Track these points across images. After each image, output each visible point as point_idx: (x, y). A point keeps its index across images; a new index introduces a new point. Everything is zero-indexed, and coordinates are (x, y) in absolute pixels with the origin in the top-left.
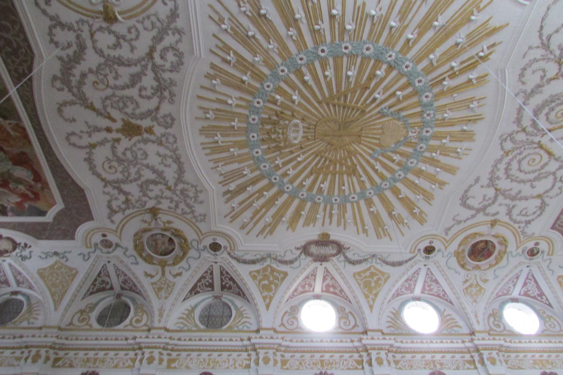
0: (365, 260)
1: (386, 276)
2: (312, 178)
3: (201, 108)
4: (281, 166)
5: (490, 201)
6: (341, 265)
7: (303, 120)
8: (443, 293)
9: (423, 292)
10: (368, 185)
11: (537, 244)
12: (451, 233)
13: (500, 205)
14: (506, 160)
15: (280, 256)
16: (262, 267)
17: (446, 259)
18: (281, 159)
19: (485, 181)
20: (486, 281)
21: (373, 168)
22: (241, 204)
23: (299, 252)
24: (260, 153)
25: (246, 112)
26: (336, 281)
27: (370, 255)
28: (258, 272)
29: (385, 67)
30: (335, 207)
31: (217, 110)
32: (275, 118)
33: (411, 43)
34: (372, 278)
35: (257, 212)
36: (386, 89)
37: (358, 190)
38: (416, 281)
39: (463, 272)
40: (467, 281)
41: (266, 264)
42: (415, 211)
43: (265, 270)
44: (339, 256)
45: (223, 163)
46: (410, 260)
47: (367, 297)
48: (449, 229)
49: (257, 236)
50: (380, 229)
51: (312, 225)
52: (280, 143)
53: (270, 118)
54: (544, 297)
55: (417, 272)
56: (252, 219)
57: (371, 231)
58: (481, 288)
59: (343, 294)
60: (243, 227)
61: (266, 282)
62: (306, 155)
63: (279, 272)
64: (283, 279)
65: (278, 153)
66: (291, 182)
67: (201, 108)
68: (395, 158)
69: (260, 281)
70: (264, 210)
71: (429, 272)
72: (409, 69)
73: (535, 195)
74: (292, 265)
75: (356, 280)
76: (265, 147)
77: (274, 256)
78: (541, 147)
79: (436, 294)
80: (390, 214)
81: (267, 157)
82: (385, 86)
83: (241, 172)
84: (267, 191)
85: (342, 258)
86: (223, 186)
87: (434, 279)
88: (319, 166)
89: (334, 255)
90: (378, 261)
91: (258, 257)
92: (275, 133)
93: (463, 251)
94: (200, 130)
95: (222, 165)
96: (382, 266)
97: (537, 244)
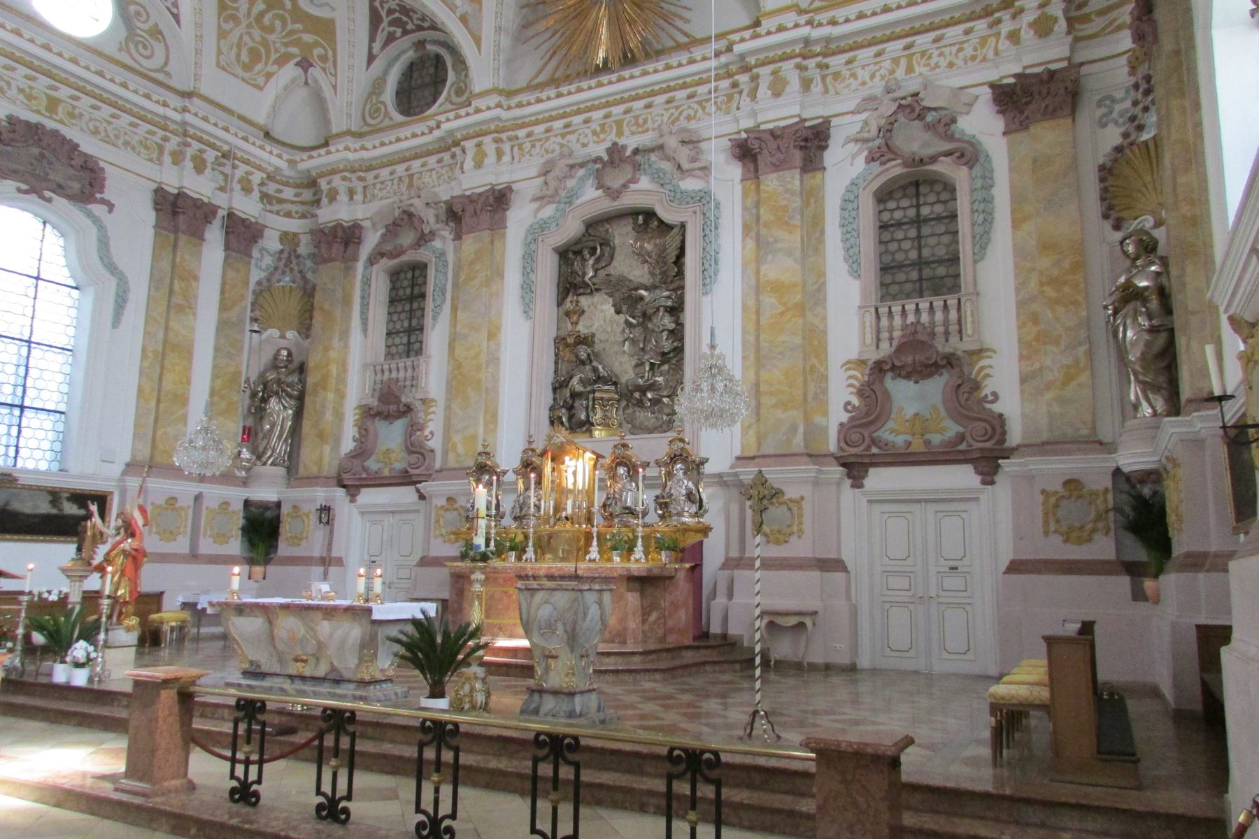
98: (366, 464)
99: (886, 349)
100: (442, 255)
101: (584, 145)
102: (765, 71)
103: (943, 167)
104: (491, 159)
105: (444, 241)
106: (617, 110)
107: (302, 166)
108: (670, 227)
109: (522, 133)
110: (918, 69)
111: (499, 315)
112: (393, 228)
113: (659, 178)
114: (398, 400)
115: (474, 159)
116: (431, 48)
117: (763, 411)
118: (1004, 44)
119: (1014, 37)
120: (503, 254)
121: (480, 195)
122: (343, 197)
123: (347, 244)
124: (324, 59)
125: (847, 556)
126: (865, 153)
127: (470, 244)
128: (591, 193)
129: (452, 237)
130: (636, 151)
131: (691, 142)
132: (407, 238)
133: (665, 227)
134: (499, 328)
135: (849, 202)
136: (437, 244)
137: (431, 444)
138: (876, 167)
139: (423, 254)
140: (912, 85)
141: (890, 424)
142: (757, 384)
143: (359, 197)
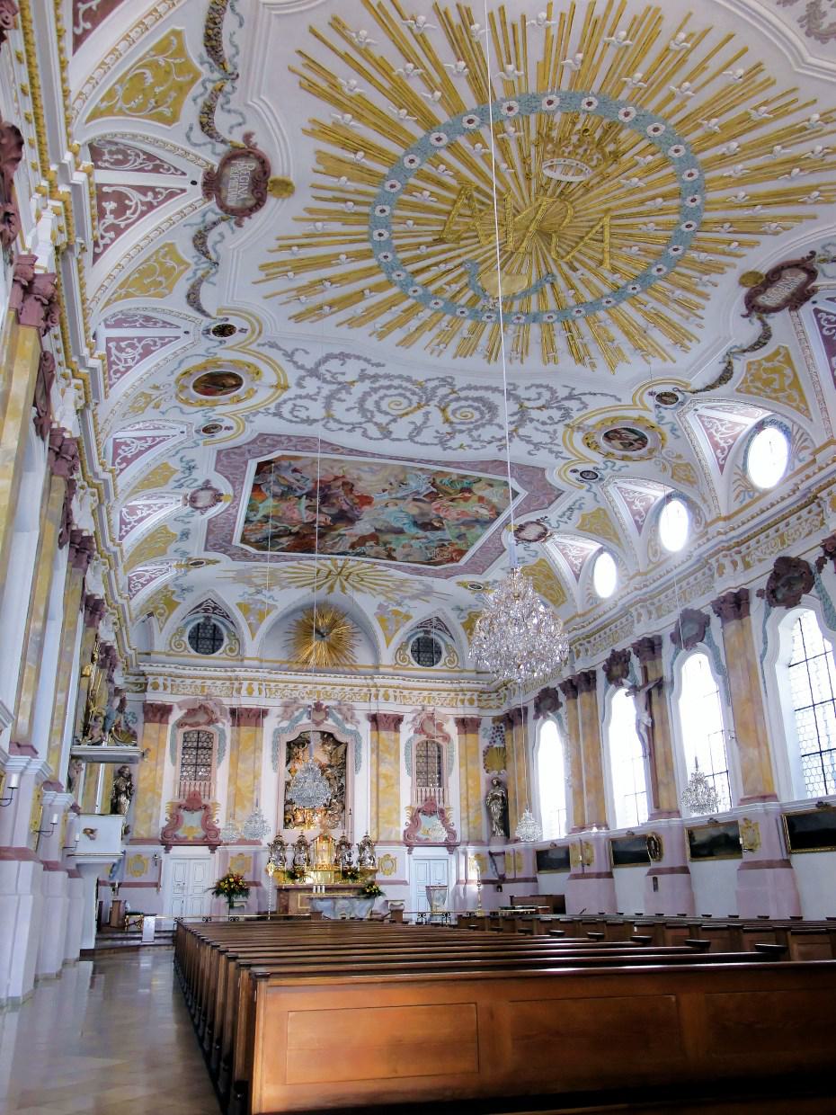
0: (206, 254)
1: (167, 291)
2: (453, 182)
3: (706, 32)
4: (499, 136)
5: (329, 379)
6: (196, 218)
7: (587, 188)
8: (123, 370)
9: (109, 340)
10: (401, 256)
11: (228, 428)
12: (266, 351)
13: (319, 388)
14: (405, 384)
15: (228, 102)
16: (196, 62)
17: (203, 353)
18: (518, 139)
19: (371, 371)
20: (156, 407)
21: (445, 261)
22: (422, 40)
23: (241, 143)
24: (545, 107)
25: (650, 107)
26: (143, 214)
27: (218, 258)
28: (181, 51)
29: (622, 283)
30: (366, 209)
31: (682, 61)
32: (610, 148)
33: (642, 307)
34: (160, 275)
35: (384, 69)
36: (586, 283)
37: (396, 242)
38: (143, 326)
39: (174, 378)
40: (156, 388)
41: (204, 71)
42: (326, 309)
43: (186, 68)
44: (218, 210)
45: (554, 32)
46: (203, 312)
47: (121, 286)
48: (273, 345)
49: (300, 52)
50: (289, 268)
51: (321, 168)
52: (555, 146)
53: (615, 141)
54: (125, 464)
55: (166, 324)
56: (365, 53)
57: (284, 256)
58: (143, 409)
59: (112, 234)
60: (337, 24)
61: (150, 80)
62: (509, 179)
63: (178, 104)
64: (161, 118)
65: (533, 136)
66: (451, 147)
67: (706, 32)
68: (453, 286)
69: (153, 66)
70: (387, 85)
71: (167, 340)
72: (605, 304)
73: (332, 412)
74: (197, 128)
75: (157, 252)
76: (558, 118)
77: (227, 88)
78: (419, 407)
79: (113, 358)
80: (330, 280)
81: (533, 118)
82: (590, 282)
83: (513, 59)
84: (442, 100)
85: (211, 217)
86: (491, 16)
87: (153, 348)
88: (475, 194)
89: (222, 206)
90: (200, 273)
91: (227, 50)
92: (579, 140)
93: (220, 366)
94: (658, 9)
95: (548, 29)
96: (188, 279)
97: (228, 428)
98: (176, 833)
99: (419, 805)
100: (222, 732)
101: (303, 698)
102: (382, 690)
103: (439, 740)
104: (256, 693)
105: (225, 725)
106: (320, 687)
107: (142, 668)
108: (341, 743)
109: (273, 684)
110: (432, 703)
111: (260, 768)
112: (192, 712)
113: (336, 720)
114: (199, 802)
115: (247, 689)
116: (213, 621)
117: (380, 824)
118: (459, 704)
119: (463, 701)
120: (262, 739)
121: (251, 709)
122: (161, 688)
123: (162, 716)
124: (161, 615)
125: (407, 879)
126: (412, 731)
127: (245, 731)
128: (305, 720)
129: (230, 723)
130: (327, 707)
131: (351, 709)
132: (202, 718)
133: (338, 743)
134: (260, 775)
135: (407, 747)
136: (220, 725)
137: (218, 826)
138: (418, 735)
139: (211, 729)
140: (430, 709)
141: (421, 831)
142: (377, 813)
143: (169, 690)
